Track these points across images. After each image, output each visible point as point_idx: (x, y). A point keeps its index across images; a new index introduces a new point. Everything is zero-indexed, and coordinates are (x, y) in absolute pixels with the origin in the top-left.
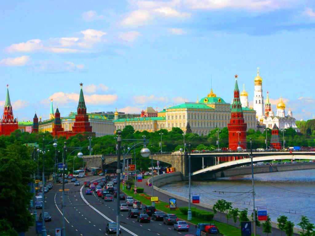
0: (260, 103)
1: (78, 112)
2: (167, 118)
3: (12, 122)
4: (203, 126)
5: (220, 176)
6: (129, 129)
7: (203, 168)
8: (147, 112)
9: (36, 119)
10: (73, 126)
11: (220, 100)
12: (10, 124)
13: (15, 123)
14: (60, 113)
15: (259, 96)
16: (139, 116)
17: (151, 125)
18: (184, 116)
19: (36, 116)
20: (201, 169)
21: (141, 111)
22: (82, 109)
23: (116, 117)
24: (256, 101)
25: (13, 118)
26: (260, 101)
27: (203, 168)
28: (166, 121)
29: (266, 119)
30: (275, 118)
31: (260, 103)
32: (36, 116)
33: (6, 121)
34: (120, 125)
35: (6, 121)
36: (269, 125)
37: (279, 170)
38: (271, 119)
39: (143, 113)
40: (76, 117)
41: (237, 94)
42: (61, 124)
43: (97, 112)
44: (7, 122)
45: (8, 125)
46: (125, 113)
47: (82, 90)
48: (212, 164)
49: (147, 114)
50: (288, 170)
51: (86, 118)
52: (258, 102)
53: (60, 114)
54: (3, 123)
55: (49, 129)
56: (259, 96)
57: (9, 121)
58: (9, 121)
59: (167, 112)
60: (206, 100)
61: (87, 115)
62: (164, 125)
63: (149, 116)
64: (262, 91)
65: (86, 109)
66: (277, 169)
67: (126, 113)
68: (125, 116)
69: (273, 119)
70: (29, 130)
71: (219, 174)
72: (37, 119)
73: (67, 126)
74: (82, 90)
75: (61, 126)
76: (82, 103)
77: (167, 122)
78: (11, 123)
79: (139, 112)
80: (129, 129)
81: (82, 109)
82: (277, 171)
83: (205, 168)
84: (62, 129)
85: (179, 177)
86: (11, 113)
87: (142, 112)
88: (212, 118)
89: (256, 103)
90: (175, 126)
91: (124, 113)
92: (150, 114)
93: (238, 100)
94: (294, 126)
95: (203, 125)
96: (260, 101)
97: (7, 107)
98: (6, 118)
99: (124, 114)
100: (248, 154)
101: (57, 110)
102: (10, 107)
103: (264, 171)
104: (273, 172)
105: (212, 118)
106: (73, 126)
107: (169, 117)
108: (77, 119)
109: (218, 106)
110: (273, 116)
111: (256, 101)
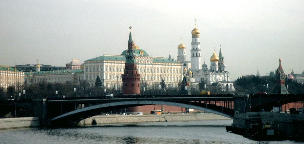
0: (197, 56)
2: (85, 70)
15: (196, 49)
20: (60, 114)
26: (197, 54)
28: (83, 74)
36: (201, 78)
38: (203, 72)
46: (52, 66)
52: (195, 55)
56: (196, 49)
66: (165, 118)
77: (85, 74)
79: (65, 66)
83: (64, 113)
85: (37, 122)
89: (193, 56)
92: (75, 67)
110: (206, 69)
111: (193, 54)
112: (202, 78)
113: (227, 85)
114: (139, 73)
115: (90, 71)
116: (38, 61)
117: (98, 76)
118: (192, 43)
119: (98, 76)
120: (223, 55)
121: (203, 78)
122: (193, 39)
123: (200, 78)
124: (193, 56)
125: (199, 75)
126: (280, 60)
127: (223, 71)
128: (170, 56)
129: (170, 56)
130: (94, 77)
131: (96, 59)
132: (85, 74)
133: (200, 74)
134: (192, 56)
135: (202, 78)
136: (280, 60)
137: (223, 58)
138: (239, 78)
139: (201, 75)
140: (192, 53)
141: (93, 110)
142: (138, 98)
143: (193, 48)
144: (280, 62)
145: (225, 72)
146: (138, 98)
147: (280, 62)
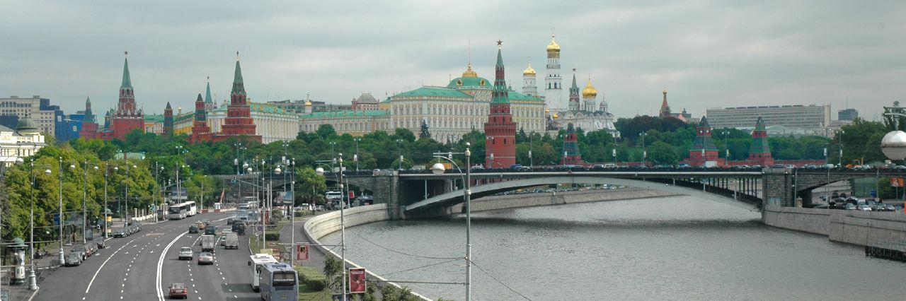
0: (555, 88)
2: (392, 113)
3: (133, 115)
4: (448, 126)
5: (460, 211)
6: (326, 131)
9: (168, 112)
10: (224, 124)
12: (131, 118)
16: (349, 108)
18: (421, 109)
19: (168, 106)
20: (424, 199)
22: (238, 96)
25: (135, 108)
26: (555, 84)
31: (555, 88)
32: (168, 106)
33: (122, 114)
35: (122, 114)
37: (567, 201)
38: (572, 115)
40: (229, 110)
41: (500, 73)
44: (125, 115)
45: (127, 120)
47: (238, 63)
48: (442, 192)
50: (584, 201)
52: (553, 86)
55: (186, 128)
57: (129, 113)
58: (129, 113)
59: (393, 101)
60: (459, 83)
61: (247, 105)
62: (387, 123)
65: (245, 97)
67: (327, 103)
68: (325, 107)
70: (157, 129)
71: (458, 208)
72: (171, 112)
73: (216, 124)
74: (238, 63)
75: (204, 125)
76: (238, 85)
77: (392, 119)
79: (350, 103)
80: (326, 131)
81: (238, 96)
82: (565, 203)
84: (208, 129)
86: (132, 100)
87: (352, 102)
89: (550, 88)
90: (399, 126)
91: (324, 103)
94: (611, 126)
95: (411, 122)
96: (555, 84)
97: (126, 89)
98: (123, 108)
100: (499, 176)
102: (130, 89)
103: (541, 203)
104: (557, 204)
106: (224, 124)
108: (230, 113)
114: (515, 120)
124: (550, 88)
126: (665, 93)
130: (415, 123)
131: (412, 93)
132: (392, 119)
133: (567, 117)
134: (548, 88)
136: (665, 93)
140: (548, 83)
144: (665, 97)
145: (608, 114)
147: (665, 97)
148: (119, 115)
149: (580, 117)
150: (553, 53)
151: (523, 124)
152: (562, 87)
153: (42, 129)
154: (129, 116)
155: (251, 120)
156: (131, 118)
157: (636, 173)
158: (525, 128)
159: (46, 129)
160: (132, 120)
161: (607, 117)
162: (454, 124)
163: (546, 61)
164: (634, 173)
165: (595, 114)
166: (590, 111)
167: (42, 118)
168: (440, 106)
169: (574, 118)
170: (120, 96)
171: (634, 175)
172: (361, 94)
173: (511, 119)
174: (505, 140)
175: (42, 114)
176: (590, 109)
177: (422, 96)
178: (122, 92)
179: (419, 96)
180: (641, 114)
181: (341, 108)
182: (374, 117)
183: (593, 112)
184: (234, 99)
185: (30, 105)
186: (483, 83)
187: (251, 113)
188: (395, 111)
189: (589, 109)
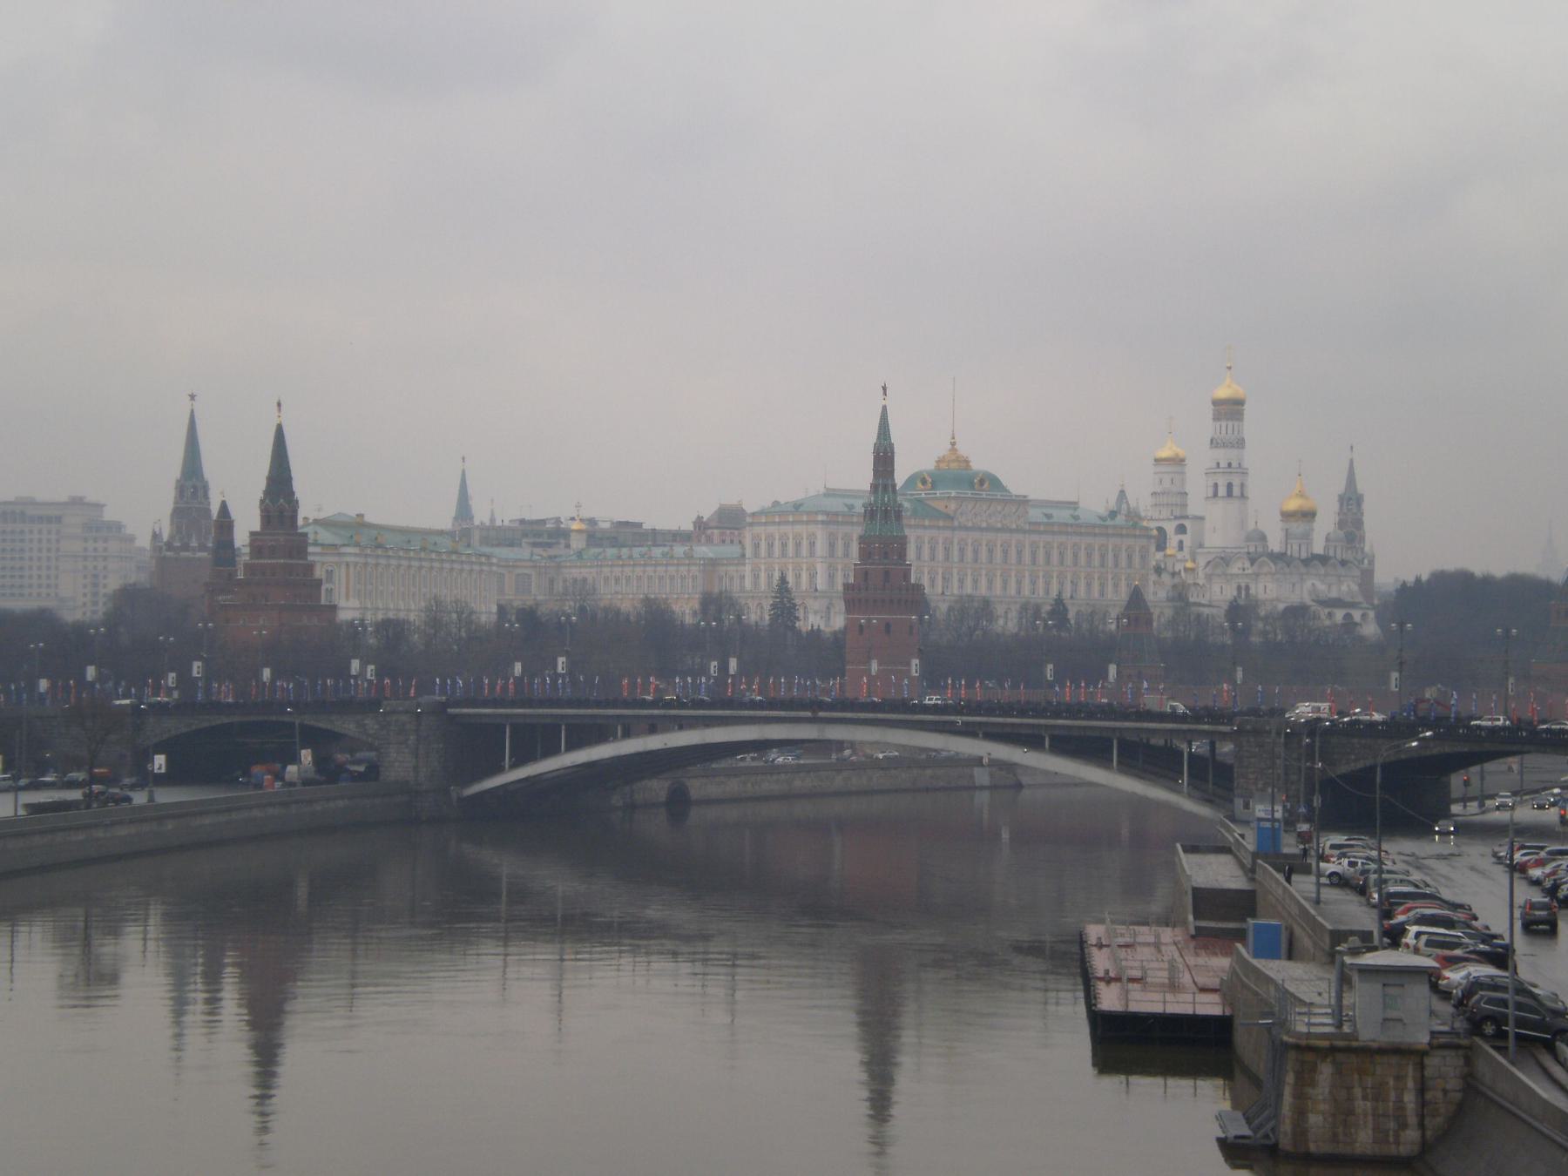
1: (263, 517)
7: (507, 766)
8: (713, 524)
11: (982, 482)
12: (199, 554)
13: (184, 554)
14: (233, 521)
15: (1230, 465)
17: (694, 578)
18: (812, 544)
20: (498, 769)
21: (694, 518)
23: (577, 543)
24: (1216, 485)
26: (1230, 486)
27: (507, 766)
29: (1227, 565)
30: (1262, 559)
31: (1230, 494)
34: (580, 573)
36: (1239, 588)
38: (1247, 564)
39: (700, 524)
42: (235, 566)
43: (527, 518)
44: (185, 547)
46: (644, 526)
49: (716, 531)
51: (299, 546)
52: (1222, 491)
53: (235, 523)
54: (168, 550)
56: (1230, 465)
57: (194, 544)
58: (194, 544)
60: (924, 482)
63: (724, 541)
64: (1240, 444)
69: (1252, 564)
77: (748, 568)
78: (199, 551)
79: (688, 526)
83: (518, 762)
87: (695, 523)
88: (940, 555)
89: (1215, 495)
92: (728, 532)
93: (885, 488)
96: (1230, 486)
99: (635, 530)
101: (224, 506)
105: (940, 555)
107: (757, 546)
109: (970, 507)
110: (1260, 550)
111: (1216, 485)
112: (1243, 585)
113: (1348, 616)
115: (769, 557)
116: (578, 506)
117: (783, 580)
118: (1212, 441)
119: (783, 580)
120: (1361, 486)
121: (1247, 588)
122: (1218, 423)
123: (1235, 586)
124: (1215, 495)
125: (1232, 575)
127: (1332, 561)
128: (1122, 492)
129: (1122, 492)
131: (797, 506)
132: (748, 568)
133: (1235, 569)
134: (1210, 494)
135: (1243, 585)
137: (1359, 500)
138: (1425, 578)
139: (1237, 575)
140: (1211, 483)
141: (639, 754)
142: (821, 714)
143: (1214, 465)
146: (821, 714)
148: (169, 545)
149: (1265, 569)
150: (1229, 409)
151: (1061, 584)
152: (1250, 492)
153: (85, 577)
154: (194, 550)
155: (310, 567)
156: (199, 554)
157: (959, 719)
158: (1067, 595)
159: (95, 576)
160: (199, 559)
161: (1342, 571)
162: (998, 583)
163: (1206, 426)
164: (952, 718)
165: (1306, 562)
166: (1297, 555)
167: (86, 549)
168: (770, 538)
169: (1250, 571)
170: (176, 503)
171: (953, 723)
172: (718, 506)
173: (906, 575)
174: (888, 626)
175: (86, 540)
176: (1296, 547)
177: (817, 513)
178: (181, 489)
179: (808, 513)
180: (1450, 564)
181: (656, 537)
182: (713, 563)
183: (1304, 555)
184: (267, 517)
185: (59, 519)
186: (982, 482)
187: (311, 549)
188: (757, 546)
189: (1293, 550)
